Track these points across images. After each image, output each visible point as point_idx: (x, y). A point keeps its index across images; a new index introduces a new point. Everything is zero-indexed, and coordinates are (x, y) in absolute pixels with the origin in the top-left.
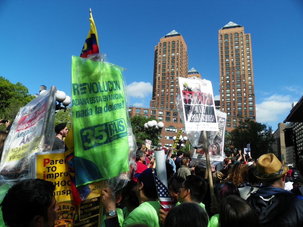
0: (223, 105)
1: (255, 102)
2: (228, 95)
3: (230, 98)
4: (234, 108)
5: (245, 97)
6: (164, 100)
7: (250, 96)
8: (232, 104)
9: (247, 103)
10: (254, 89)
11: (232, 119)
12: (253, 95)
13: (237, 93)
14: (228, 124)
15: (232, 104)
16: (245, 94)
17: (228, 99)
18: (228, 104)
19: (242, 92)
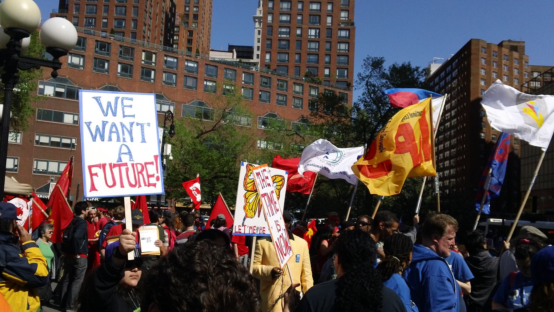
0: (268, 44)
1: (354, 44)
2: (284, 18)
3: (289, 27)
4: (297, 57)
5: (329, 29)
6: (96, 13)
7: (342, 26)
8: (293, 45)
9: (333, 44)
10: (353, 8)
11: (290, 83)
12: (350, 25)
13: (310, 15)
14: (281, 98)
15: (293, 45)
16: (329, 20)
17: (284, 30)
18: (284, 43)
19: (323, 14)
